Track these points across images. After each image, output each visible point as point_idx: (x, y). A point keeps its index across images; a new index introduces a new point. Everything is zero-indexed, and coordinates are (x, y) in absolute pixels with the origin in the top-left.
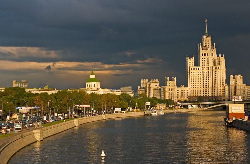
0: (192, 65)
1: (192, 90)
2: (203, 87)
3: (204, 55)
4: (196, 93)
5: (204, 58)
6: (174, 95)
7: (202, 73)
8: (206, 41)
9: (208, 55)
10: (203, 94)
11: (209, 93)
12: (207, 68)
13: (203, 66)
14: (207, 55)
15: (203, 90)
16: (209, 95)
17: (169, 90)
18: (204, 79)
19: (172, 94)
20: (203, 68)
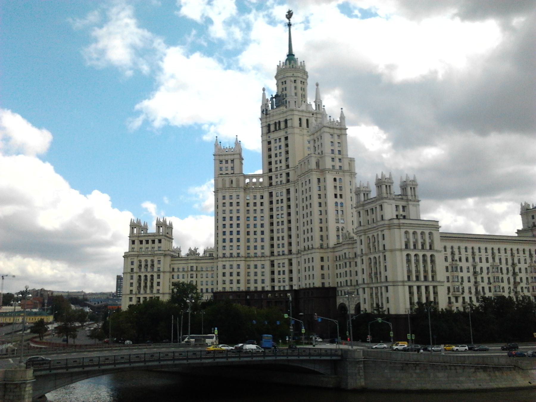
0: (230, 172)
1: (224, 267)
2: (272, 253)
3: (272, 128)
4: (242, 278)
5: (273, 142)
6: (155, 287)
7: (266, 200)
8: (283, 80)
9: (286, 126)
10: (273, 280)
11: (291, 279)
12: (284, 175)
13: (270, 170)
14: (283, 125)
15: (273, 265)
16: (291, 286)
17: (135, 267)
18: (275, 220)
19: (149, 284)
20: (271, 178)
